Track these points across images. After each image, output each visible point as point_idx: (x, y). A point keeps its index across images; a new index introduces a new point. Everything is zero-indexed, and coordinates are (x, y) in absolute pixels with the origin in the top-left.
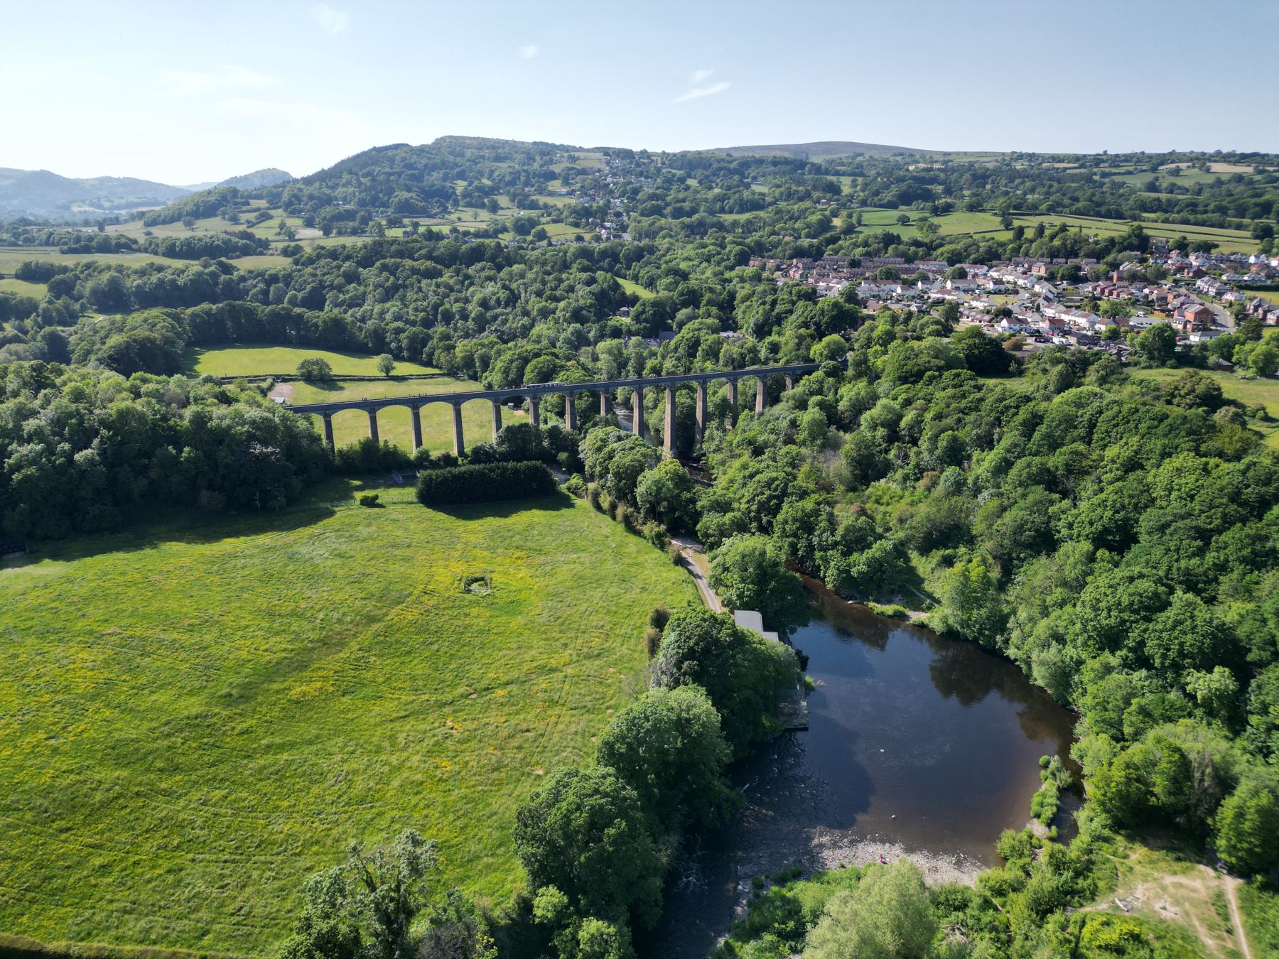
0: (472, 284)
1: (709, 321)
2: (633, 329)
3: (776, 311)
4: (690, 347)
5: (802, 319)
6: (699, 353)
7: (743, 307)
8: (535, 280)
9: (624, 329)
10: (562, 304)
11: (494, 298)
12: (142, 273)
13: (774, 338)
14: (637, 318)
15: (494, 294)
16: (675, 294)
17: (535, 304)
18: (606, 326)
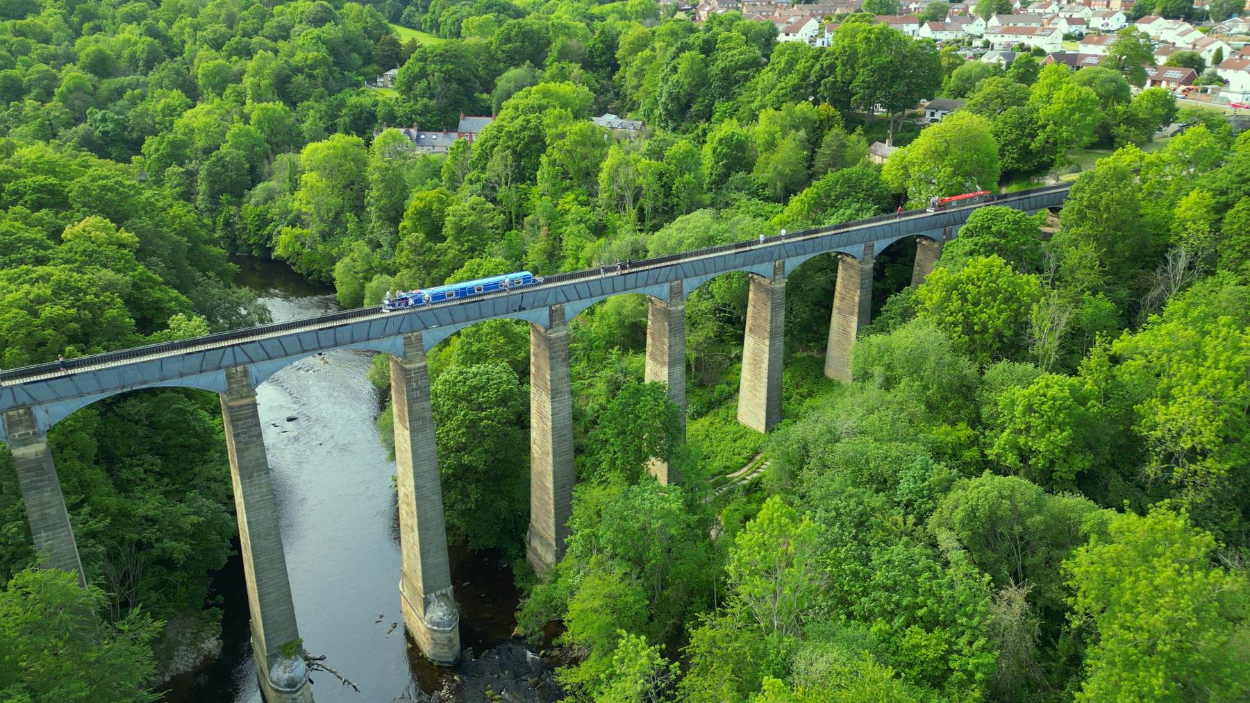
0: (97, 29)
2: (399, 112)
3: (720, 64)
4: (517, 155)
5: (792, 79)
7: (637, 61)
8: (214, 18)
9: (380, 111)
10: (251, 65)
11: (126, 53)
13: (725, 128)
14: (408, 87)
15: (127, 42)
17: (205, 62)
18: (342, 104)
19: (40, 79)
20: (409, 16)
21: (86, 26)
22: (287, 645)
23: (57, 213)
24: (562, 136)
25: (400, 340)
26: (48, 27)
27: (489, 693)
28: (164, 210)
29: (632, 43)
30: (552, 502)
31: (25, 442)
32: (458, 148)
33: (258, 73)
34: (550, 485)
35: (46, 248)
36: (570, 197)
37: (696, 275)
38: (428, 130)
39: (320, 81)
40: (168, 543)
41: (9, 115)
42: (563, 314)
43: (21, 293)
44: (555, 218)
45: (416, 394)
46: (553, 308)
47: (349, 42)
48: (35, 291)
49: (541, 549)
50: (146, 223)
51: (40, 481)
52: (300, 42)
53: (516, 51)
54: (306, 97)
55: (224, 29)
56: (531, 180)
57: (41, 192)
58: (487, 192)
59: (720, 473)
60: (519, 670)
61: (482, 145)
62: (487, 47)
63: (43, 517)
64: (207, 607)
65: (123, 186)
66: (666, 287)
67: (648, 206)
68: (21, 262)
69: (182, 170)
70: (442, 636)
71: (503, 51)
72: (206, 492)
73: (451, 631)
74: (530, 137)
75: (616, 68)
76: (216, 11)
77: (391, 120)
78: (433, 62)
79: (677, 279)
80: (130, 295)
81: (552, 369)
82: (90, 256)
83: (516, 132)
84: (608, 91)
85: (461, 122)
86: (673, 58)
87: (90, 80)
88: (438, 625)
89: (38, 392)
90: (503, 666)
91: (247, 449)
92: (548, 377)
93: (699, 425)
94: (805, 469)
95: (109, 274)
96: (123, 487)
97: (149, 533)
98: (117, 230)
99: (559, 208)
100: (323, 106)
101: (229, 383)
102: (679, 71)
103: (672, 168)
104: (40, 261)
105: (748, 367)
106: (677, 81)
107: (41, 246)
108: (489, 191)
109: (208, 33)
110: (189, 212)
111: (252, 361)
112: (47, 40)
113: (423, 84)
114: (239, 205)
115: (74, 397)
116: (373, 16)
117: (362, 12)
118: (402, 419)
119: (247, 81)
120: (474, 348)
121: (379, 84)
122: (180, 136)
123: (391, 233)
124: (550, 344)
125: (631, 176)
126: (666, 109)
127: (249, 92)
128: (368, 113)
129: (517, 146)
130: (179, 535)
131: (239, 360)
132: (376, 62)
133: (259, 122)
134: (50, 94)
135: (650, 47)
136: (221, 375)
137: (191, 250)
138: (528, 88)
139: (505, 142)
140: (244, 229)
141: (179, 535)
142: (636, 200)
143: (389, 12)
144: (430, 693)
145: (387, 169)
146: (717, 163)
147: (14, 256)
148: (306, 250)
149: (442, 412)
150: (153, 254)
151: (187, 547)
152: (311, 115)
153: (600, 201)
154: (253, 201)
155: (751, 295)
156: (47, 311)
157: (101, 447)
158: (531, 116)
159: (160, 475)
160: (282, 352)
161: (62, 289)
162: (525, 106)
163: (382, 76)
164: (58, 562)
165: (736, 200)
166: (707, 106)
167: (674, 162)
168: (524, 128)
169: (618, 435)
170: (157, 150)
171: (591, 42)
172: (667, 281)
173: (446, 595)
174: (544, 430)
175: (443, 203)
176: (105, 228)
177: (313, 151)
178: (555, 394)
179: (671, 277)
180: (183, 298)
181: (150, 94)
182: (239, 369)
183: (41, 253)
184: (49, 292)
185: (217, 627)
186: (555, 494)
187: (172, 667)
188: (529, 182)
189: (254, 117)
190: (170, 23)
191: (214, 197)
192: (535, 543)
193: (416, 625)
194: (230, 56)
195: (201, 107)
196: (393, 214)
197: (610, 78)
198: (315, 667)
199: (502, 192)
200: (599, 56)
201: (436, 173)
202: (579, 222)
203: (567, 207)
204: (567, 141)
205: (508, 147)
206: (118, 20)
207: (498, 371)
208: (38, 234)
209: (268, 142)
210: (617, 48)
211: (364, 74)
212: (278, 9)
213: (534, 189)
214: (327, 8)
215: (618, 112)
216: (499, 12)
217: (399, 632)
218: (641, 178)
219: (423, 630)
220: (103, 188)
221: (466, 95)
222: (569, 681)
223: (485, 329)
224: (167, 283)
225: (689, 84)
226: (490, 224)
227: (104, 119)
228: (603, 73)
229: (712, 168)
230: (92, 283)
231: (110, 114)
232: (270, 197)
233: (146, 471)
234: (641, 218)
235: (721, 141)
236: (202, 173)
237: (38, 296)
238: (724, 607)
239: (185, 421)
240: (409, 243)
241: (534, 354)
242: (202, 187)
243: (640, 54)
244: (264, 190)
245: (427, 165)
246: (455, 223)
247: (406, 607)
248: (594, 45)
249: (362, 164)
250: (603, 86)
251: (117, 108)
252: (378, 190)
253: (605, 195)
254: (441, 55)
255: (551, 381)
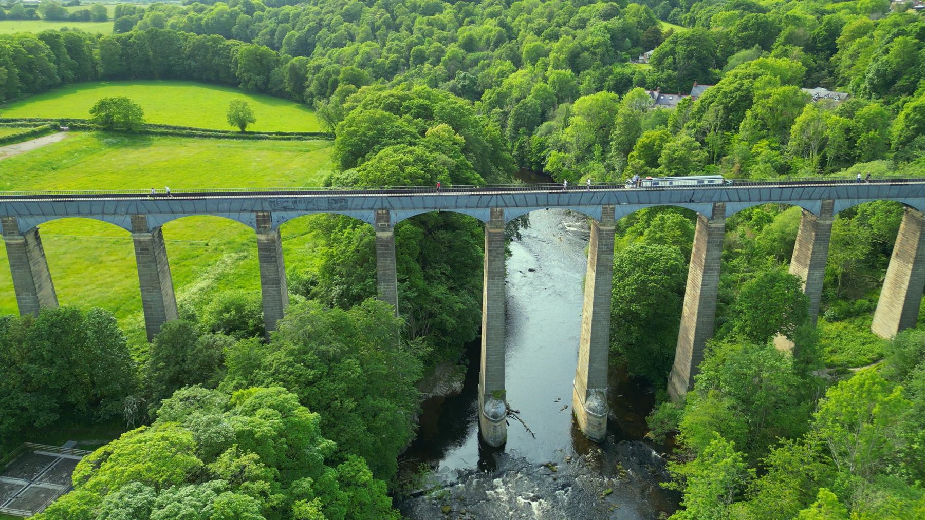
0: (472, 22)
1: (783, 63)
2: (649, 79)
4: (727, 110)
6: (747, 123)
7: (854, 46)
8: (541, 15)
9: (636, 78)
10: (556, 45)
11: (485, 37)
12: (185, 13)
14: (659, 62)
16: (733, 29)
18: (610, 72)
19: (435, 52)
20: (675, 15)
21: (466, 20)
22: (497, 392)
23: (426, 121)
24: (768, 96)
25: (600, 208)
26: (445, 21)
27: (619, 467)
28: (483, 127)
29: (851, 31)
30: (691, 350)
31: (383, 229)
32: (684, 103)
33: (560, 50)
34: (692, 338)
35: (416, 138)
36: (765, 142)
37: (849, 198)
38: (668, 93)
39: (599, 56)
40: (445, 316)
41: (416, 73)
42: (724, 211)
43: (399, 158)
44: (747, 159)
45: (604, 248)
46: (717, 205)
47: (625, 31)
48: (405, 158)
49: (678, 386)
50: (472, 132)
51: (387, 253)
52: (592, 29)
53: (749, 37)
54: (587, 67)
55: (545, 22)
56: (735, 129)
57: (420, 108)
58: (699, 136)
59: (842, 365)
60: (644, 459)
61: (702, 101)
62: (727, 34)
63: (385, 274)
64: (459, 364)
65: (464, 109)
66: (818, 204)
67: (830, 153)
68: (403, 143)
69: (501, 111)
70: (594, 419)
71: (739, 38)
72: (471, 293)
73: (601, 418)
74: (741, 96)
75: (835, 51)
76: (543, 10)
77: (642, 83)
78: (681, 44)
79: (829, 198)
80: (453, 172)
81: (708, 251)
82: (437, 146)
83: (731, 93)
84: (824, 70)
85: (694, 89)
86: (888, 43)
87: (462, 53)
88: (593, 411)
89: (395, 202)
90: (633, 455)
91: (494, 260)
92: (704, 256)
93: (834, 327)
94: (916, 369)
95: (444, 157)
96: (428, 279)
97: (436, 308)
98: (455, 135)
99: (753, 150)
100: (597, 74)
101: (492, 218)
102: (891, 53)
103: (860, 125)
104: (411, 144)
105: (889, 286)
106: (887, 61)
107: (414, 136)
108: (701, 135)
109: (535, 25)
110: (497, 130)
111: (507, 206)
112: (443, 29)
113: (670, 59)
114: (530, 135)
115: (411, 209)
116: (647, 13)
117: (638, 10)
118: (592, 265)
119: (552, 55)
120: (657, 236)
121: (640, 61)
122: (505, 90)
123: (624, 161)
124: (709, 231)
125: (820, 129)
126: (871, 84)
127: (552, 63)
128: (627, 79)
129: (729, 103)
130: (452, 313)
131: (499, 204)
132: (642, 46)
133: (554, 82)
134: (439, 61)
135: (869, 35)
136: (488, 211)
137: (494, 152)
138: (749, 62)
139: (720, 100)
140: (530, 151)
141: (452, 313)
142: (820, 149)
143: (660, 12)
144: (580, 454)
145: (629, 115)
146: (908, 127)
147: (399, 140)
148: (565, 168)
149: (625, 271)
150: (471, 151)
151: (454, 322)
152: (588, 78)
153: (789, 148)
154: (539, 133)
155: (902, 225)
156: (409, 169)
157: (421, 253)
158: (745, 81)
159: (448, 277)
160: (525, 204)
161: (419, 160)
162: (743, 74)
163: (643, 55)
164: (385, 298)
165: (917, 156)
166: (912, 82)
167: (862, 120)
168: (737, 90)
169: (751, 308)
170: (490, 98)
171: (816, 31)
172: (820, 198)
173: (602, 393)
174: (695, 297)
175: (663, 140)
176: (449, 132)
177: (585, 102)
178: (707, 270)
179: (825, 195)
180: (482, 179)
181: (493, 64)
182: (499, 209)
183: (413, 140)
184: (412, 160)
185: (462, 376)
186: (695, 345)
187: (434, 391)
188: (733, 131)
189: (551, 79)
190: (514, 18)
191: (516, 129)
192: (675, 380)
193: (579, 409)
194: (544, 40)
195: (521, 72)
196: (627, 148)
197: (828, 59)
198: (512, 416)
199: (710, 137)
200: (821, 42)
201: (664, 122)
202: (766, 162)
203: (760, 150)
204: (770, 100)
205: (722, 103)
206: (484, 17)
207: (671, 251)
208: (412, 129)
209: (557, 96)
210: (839, 36)
211: (631, 54)
212: (583, 8)
213: (735, 136)
214: (615, 7)
215: (829, 87)
216: (744, 9)
217: (568, 412)
218: (829, 131)
219: (583, 412)
220: (453, 109)
221: (702, 69)
222: (675, 471)
223: (668, 223)
224: (476, 171)
225: (898, 63)
226: (696, 159)
227: (464, 78)
228: (822, 55)
229: (902, 131)
230: (435, 159)
231: (468, 74)
232: (550, 132)
233: (442, 273)
234: (823, 163)
235: (915, 109)
236: (512, 113)
237: (406, 161)
238: (803, 439)
239: (467, 248)
240: (632, 166)
241: (697, 239)
242: (510, 122)
243: (857, 40)
244: (547, 127)
245: (659, 116)
246: (669, 154)
247: (575, 396)
248: (818, 33)
249: (613, 112)
250: (819, 65)
251: (473, 71)
252: (620, 130)
253: (794, 143)
254: (688, 39)
255: (706, 259)
